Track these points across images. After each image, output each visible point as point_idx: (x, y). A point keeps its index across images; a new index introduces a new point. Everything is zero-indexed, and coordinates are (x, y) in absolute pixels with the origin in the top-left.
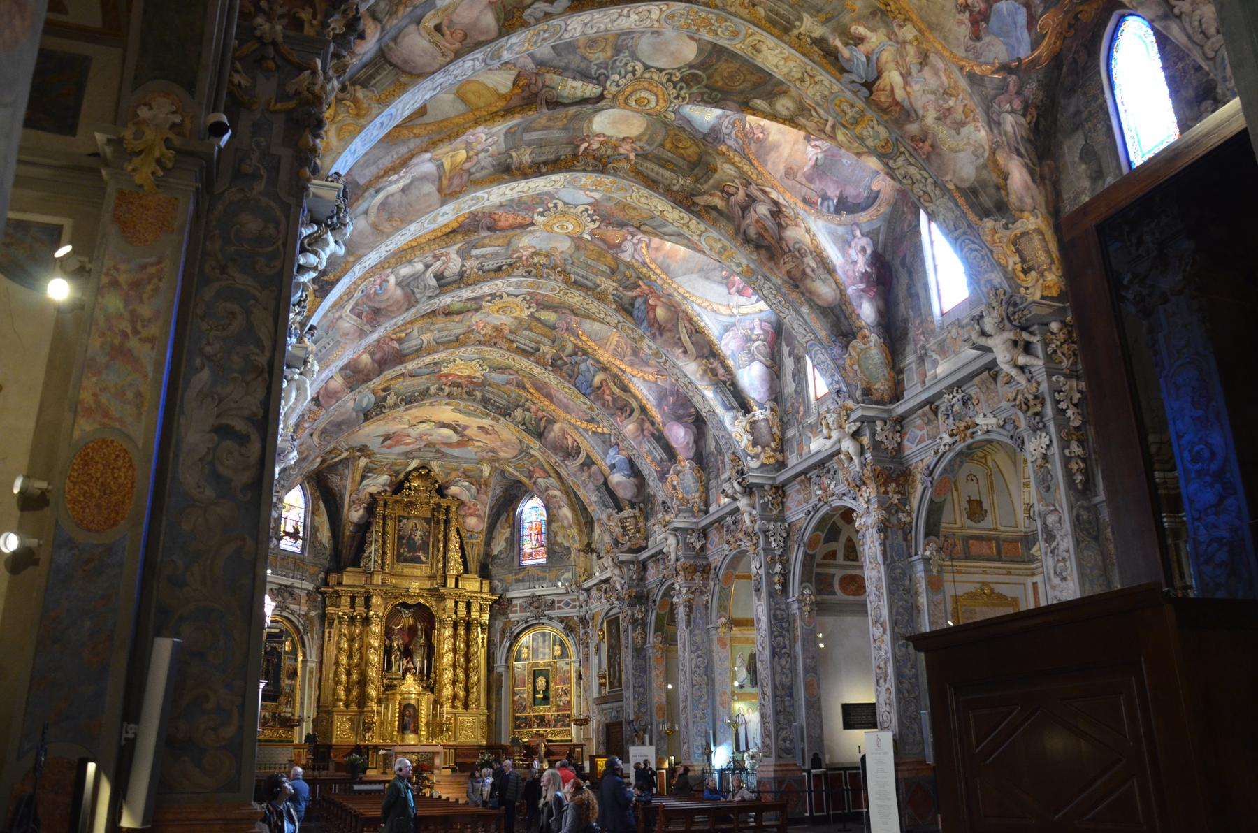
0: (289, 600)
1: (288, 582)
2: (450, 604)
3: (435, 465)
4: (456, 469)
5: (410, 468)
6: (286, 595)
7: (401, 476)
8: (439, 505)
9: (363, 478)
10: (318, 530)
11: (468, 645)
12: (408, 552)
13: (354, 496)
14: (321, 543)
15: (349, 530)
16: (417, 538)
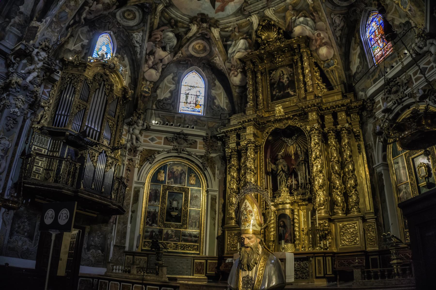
0: (185, 144)
1: (178, 130)
2: (313, 116)
3: (269, 13)
4: (286, 10)
5: (255, 26)
6: (182, 141)
7: (254, 36)
8: (291, 48)
9: (226, 47)
10: (215, 98)
11: (341, 153)
12: (280, 92)
13: (227, 64)
14: (219, 107)
15: (236, 92)
16: (285, 80)
